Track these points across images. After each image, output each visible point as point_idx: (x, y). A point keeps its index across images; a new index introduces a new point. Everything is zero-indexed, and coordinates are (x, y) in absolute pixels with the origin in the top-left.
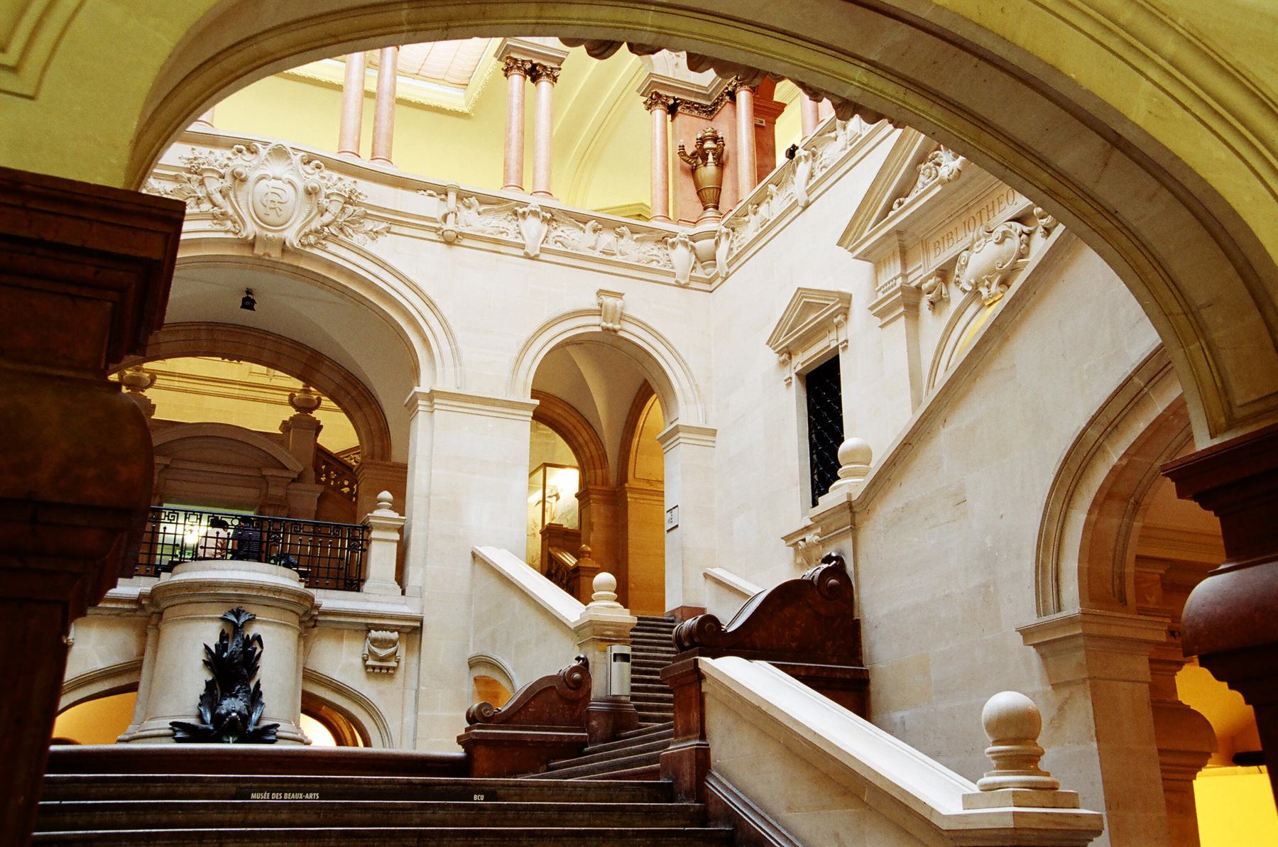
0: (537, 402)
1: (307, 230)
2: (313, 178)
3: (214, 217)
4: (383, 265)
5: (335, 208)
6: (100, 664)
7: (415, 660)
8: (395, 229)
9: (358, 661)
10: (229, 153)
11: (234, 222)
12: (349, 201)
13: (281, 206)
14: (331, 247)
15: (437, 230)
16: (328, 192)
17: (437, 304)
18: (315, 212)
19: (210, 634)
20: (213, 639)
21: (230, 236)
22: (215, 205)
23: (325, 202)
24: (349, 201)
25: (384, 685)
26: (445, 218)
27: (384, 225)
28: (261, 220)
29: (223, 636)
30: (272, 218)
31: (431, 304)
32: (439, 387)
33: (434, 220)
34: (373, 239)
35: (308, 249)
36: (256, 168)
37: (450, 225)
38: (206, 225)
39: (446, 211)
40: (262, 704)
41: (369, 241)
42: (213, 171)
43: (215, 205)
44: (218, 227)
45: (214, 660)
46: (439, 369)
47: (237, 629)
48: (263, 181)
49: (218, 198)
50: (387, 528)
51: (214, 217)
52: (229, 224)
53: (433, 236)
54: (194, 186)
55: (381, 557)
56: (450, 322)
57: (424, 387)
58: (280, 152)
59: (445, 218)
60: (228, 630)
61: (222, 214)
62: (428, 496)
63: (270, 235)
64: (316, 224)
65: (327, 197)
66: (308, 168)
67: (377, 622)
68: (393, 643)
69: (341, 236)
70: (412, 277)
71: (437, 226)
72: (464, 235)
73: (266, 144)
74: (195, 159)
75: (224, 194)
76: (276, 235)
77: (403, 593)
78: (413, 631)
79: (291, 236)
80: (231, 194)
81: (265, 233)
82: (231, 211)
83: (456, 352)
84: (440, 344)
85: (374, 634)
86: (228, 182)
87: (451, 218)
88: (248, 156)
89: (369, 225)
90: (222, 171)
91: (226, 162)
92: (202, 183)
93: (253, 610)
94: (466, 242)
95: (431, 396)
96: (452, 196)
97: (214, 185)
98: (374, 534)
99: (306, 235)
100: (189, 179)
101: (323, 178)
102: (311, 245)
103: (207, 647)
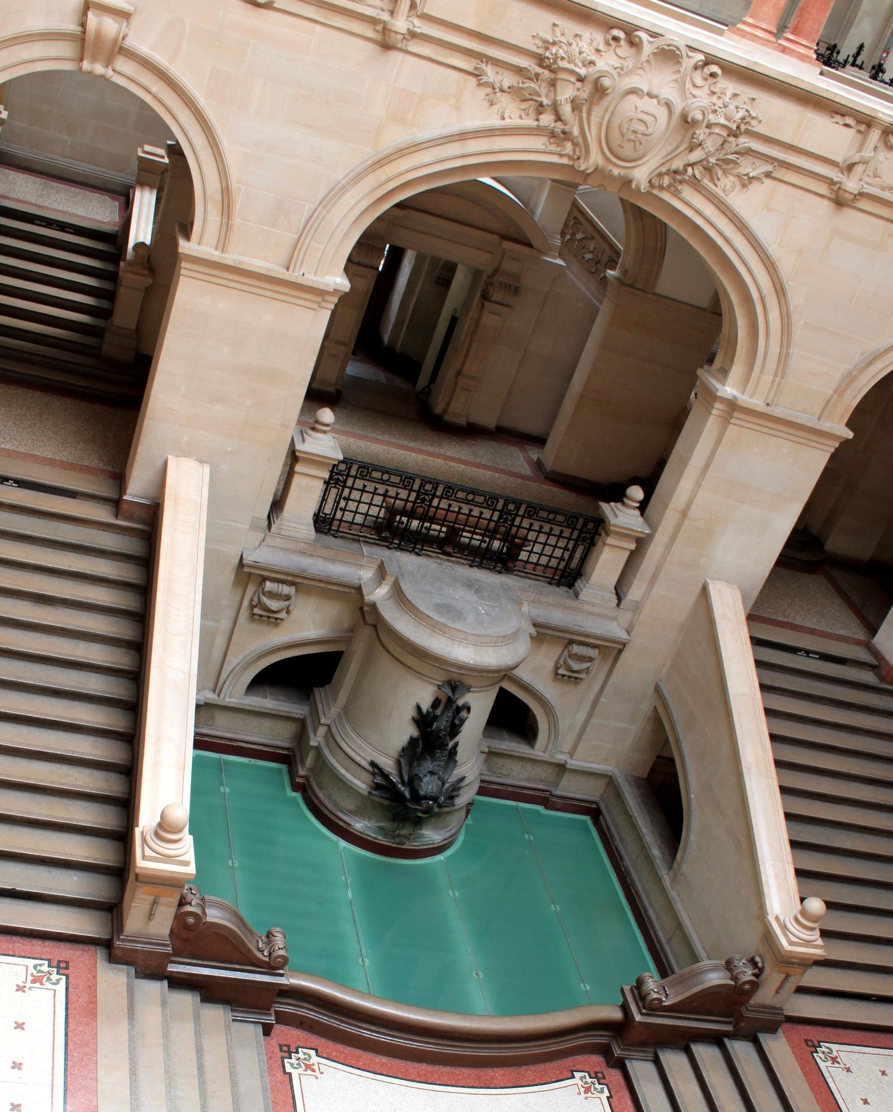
0: (850, 435)
1: (664, 170)
2: (700, 100)
3: (553, 135)
4: (742, 227)
5: (711, 145)
6: (312, 633)
7: (606, 668)
8: (781, 173)
9: (550, 665)
10: (599, 38)
11: (575, 144)
12: (734, 134)
13: (643, 139)
14: (688, 193)
15: (831, 182)
16: (712, 118)
17: (790, 294)
18: (684, 146)
19: (424, 695)
20: (425, 707)
21: (565, 161)
22: (559, 118)
23: (701, 133)
24: (734, 134)
25: (567, 688)
26: (850, 167)
27: (769, 168)
28: (612, 150)
29: (436, 704)
30: (628, 151)
31: (780, 291)
32: (745, 399)
33: (834, 164)
34: (744, 186)
35: (655, 192)
36: (628, 74)
37: (852, 185)
38: (538, 142)
39: (856, 159)
40: (456, 762)
41: (738, 187)
42: (572, 72)
43: (559, 118)
44: (553, 148)
45: (423, 720)
46: (755, 374)
47: (450, 701)
48: (633, 98)
49: (566, 110)
50: (624, 536)
51: (553, 135)
52: (569, 147)
53: (823, 189)
54: (543, 89)
55: (607, 562)
56: (794, 318)
57: (728, 389)
58: (669, 55)
59: (850, 167)
60: (444, 700)
61: (564, 133)
62: (684, 514)
63: (616, 171)
64: (678, 164)
65: (709, 126)
66: (698, 78)
67: (582, 639)
68: (591, 659)
69: (706, 182)
70: (773, 250)
71: (835, 175)
72: (861, 194)
73: (654, 35)
74: (554, 43)
75: (576, 105)
76: (623, 172)
77: (618, 605)
78: (613, 651)
79: (641, 175)
80: (585, 109)
81: (610, 167)
82: (576, 131)
83: (784, 358)
84: (770, 344)
85: (576, 649)
86: (585, 93)
87: (859, 169)
88: (624, 49)
89: (747, 167)
90: (582, 72)
91: (593, 57)
92: (553, 84)
93: (469, 681)
94: (863, 204)
95: (732, 406)
96: (875, 135)
97: (566, 92)
98: (610, 540)
99: (660, 175)
100: (537, 76)
101: (713, 93)
102: (661, 188)
103: (419, 708)
